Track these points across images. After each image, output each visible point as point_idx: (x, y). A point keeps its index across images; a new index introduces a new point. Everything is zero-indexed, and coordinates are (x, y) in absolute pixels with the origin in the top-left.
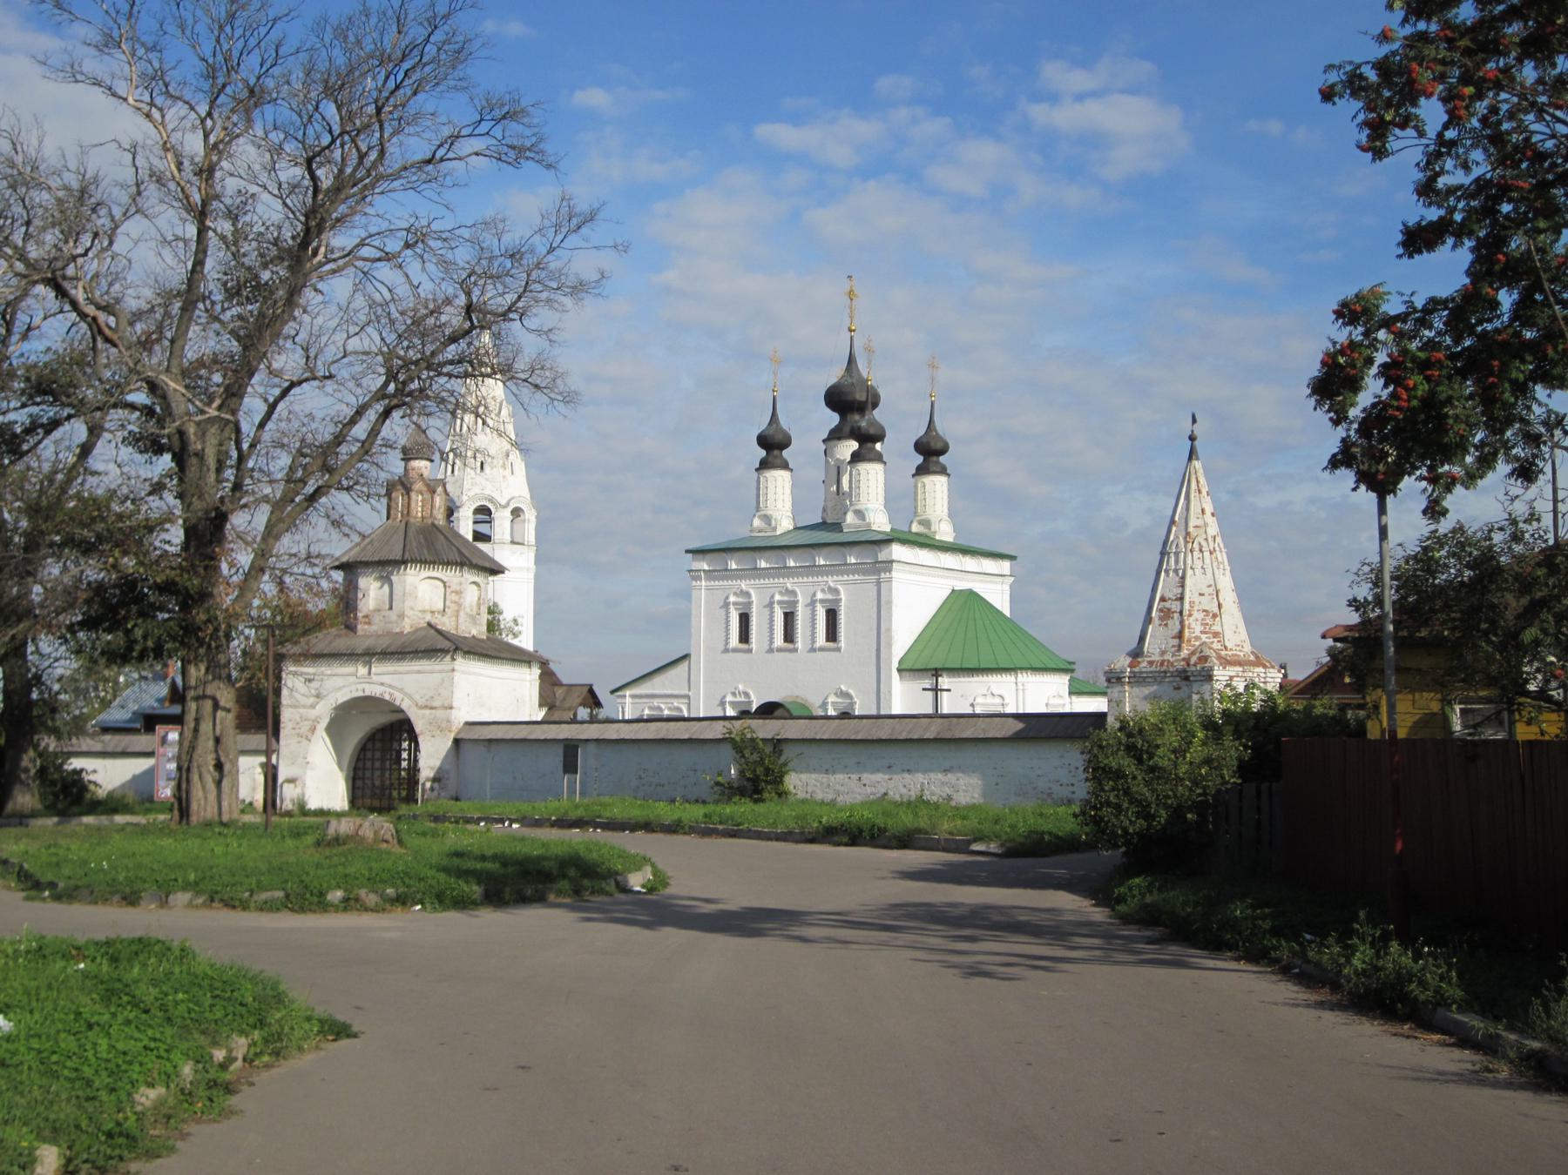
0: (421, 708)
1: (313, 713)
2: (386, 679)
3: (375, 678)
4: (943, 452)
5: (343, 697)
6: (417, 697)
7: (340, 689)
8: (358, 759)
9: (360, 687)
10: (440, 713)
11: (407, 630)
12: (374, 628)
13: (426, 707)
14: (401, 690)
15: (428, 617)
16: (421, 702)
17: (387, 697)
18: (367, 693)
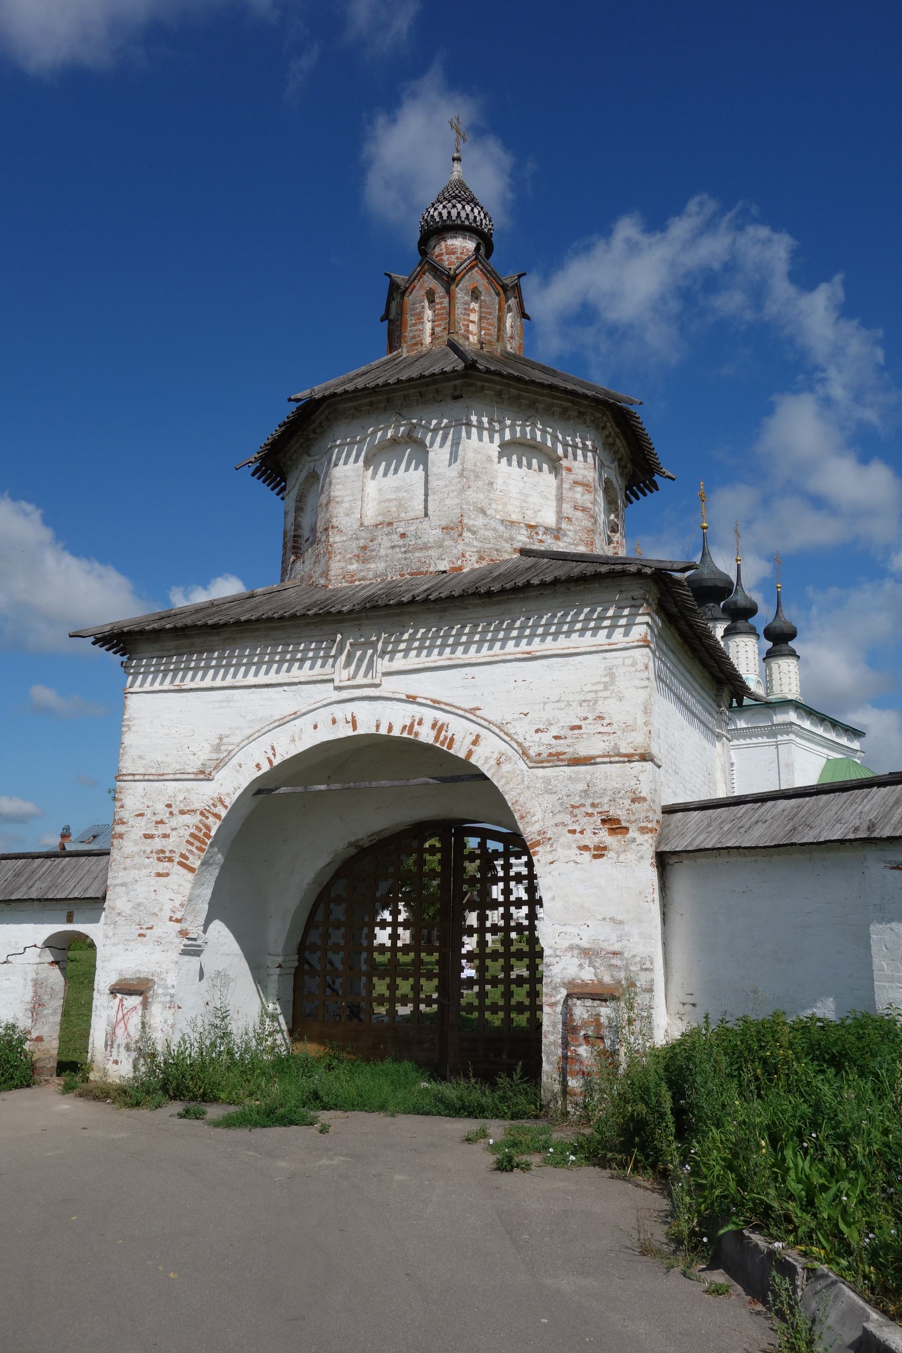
0: (538, 762)
1: (203, 794)
2: (425, 686)
3: (390, 686)
4: (792, 635)
5: (290, 744)
6: (522, 730)
7: (283, 722)
8: (310, 923)
9: (343, 712)
10: (610, 777)
11: (471, 564)
12: (378, 566)
13: (555, 759)
14: (471, 714)
15: (522, 539)
16: (538, 744)
17: (426, 735)
18: (365, 728)
